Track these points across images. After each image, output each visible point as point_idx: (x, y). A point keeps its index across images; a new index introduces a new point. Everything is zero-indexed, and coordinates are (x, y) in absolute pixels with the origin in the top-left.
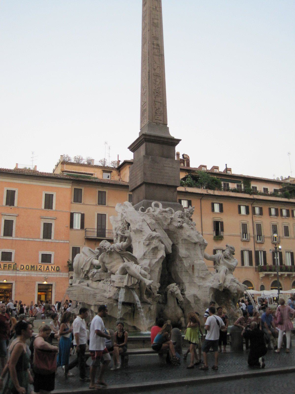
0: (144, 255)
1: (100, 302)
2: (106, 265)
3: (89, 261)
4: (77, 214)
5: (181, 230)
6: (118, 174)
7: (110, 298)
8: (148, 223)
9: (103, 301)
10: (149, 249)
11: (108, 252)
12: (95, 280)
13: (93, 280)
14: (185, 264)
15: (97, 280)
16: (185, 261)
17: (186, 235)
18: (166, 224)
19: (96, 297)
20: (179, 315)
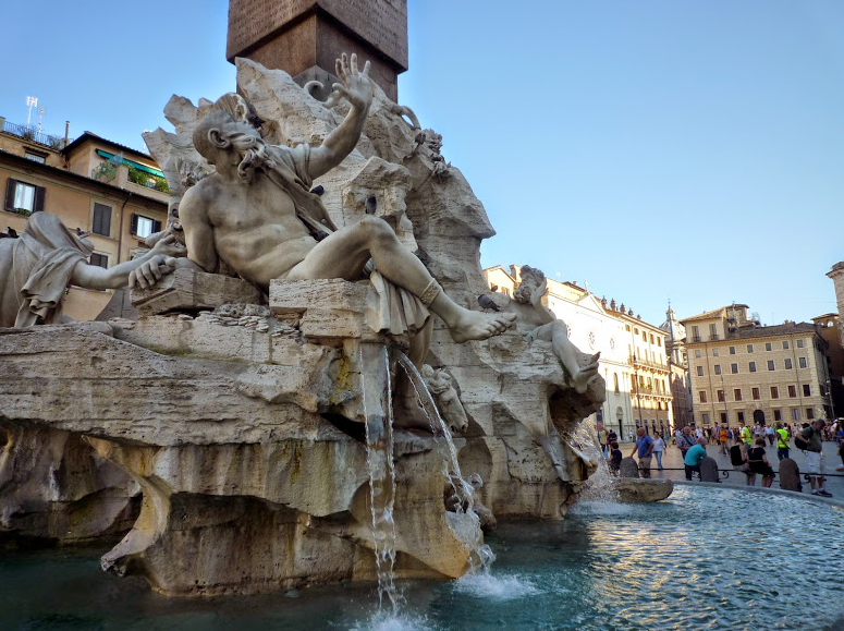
3: (60, 264)
5: (438, 189)
7: (283, 401)
9: (234, 420)
13: (150, 307)
15: (175, 305)
19: (189, 398)
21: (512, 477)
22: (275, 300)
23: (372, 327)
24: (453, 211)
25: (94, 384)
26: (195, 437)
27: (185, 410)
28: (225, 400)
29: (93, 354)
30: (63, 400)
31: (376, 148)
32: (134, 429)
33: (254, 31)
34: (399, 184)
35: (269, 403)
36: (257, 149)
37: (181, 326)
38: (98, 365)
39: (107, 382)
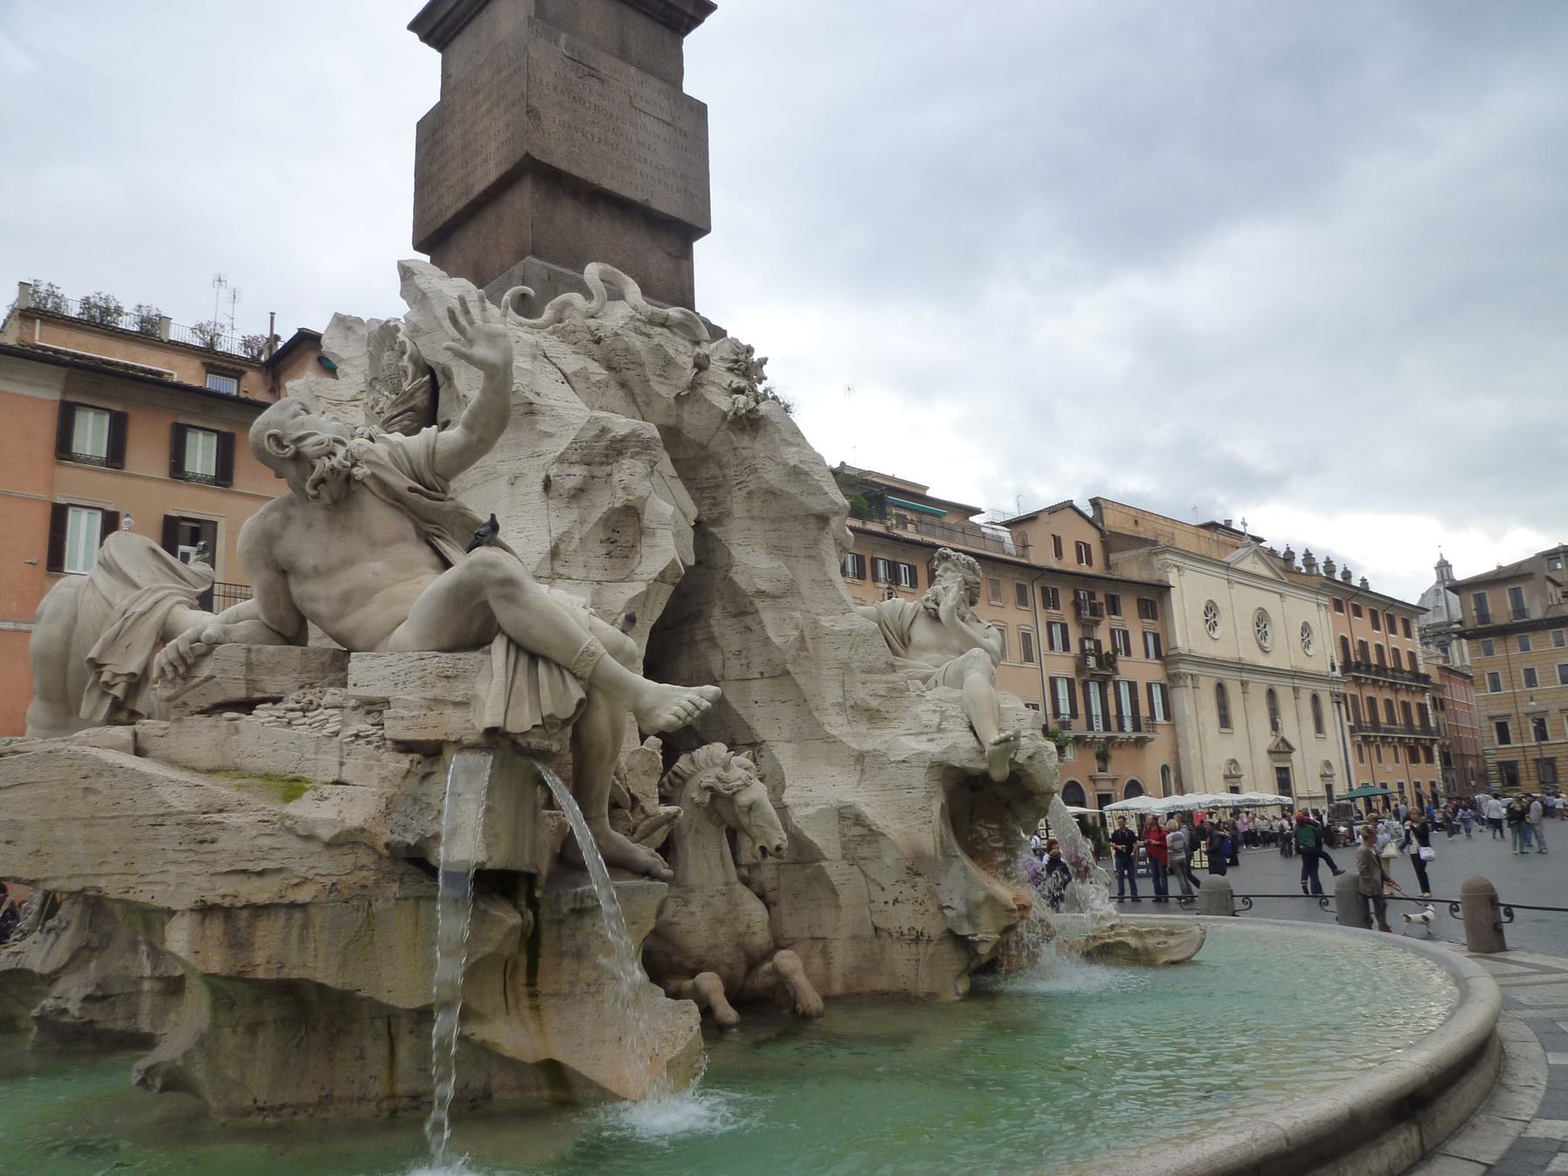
0: (554, 553)
1: (256, 882)
2: (301, 590)
3: (144, 614)
4: (85, 513)
5: (744, 441)
6: (269, 387)
7: (346, 841)
8: (568, 372)
9: (279, 870)
10: (583, 522)
11: (322, 481)
12: (206, 705)
14: (771, 633)
16: (767, 617)
17: (778, 464)
18: (666, 391)
20: (754, 933)
21: (876, 929)
22: (355, 685)
23: (477, 724)
24: (768, 476)
25: (86, 826)
26: (224, 896)
27: (211, 857)
28: (266, 842)
29: (85, 783)
30: (45, 849)
31: (623, 385)
32: (140, 888)
33: (447, 201)
34: (637, 454)
35: (330, 845)
36: (334, 454)
37: (224, 730)
38: (91, 798)
39: (103, 822)
